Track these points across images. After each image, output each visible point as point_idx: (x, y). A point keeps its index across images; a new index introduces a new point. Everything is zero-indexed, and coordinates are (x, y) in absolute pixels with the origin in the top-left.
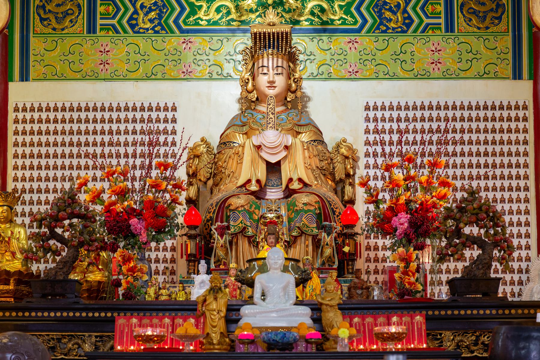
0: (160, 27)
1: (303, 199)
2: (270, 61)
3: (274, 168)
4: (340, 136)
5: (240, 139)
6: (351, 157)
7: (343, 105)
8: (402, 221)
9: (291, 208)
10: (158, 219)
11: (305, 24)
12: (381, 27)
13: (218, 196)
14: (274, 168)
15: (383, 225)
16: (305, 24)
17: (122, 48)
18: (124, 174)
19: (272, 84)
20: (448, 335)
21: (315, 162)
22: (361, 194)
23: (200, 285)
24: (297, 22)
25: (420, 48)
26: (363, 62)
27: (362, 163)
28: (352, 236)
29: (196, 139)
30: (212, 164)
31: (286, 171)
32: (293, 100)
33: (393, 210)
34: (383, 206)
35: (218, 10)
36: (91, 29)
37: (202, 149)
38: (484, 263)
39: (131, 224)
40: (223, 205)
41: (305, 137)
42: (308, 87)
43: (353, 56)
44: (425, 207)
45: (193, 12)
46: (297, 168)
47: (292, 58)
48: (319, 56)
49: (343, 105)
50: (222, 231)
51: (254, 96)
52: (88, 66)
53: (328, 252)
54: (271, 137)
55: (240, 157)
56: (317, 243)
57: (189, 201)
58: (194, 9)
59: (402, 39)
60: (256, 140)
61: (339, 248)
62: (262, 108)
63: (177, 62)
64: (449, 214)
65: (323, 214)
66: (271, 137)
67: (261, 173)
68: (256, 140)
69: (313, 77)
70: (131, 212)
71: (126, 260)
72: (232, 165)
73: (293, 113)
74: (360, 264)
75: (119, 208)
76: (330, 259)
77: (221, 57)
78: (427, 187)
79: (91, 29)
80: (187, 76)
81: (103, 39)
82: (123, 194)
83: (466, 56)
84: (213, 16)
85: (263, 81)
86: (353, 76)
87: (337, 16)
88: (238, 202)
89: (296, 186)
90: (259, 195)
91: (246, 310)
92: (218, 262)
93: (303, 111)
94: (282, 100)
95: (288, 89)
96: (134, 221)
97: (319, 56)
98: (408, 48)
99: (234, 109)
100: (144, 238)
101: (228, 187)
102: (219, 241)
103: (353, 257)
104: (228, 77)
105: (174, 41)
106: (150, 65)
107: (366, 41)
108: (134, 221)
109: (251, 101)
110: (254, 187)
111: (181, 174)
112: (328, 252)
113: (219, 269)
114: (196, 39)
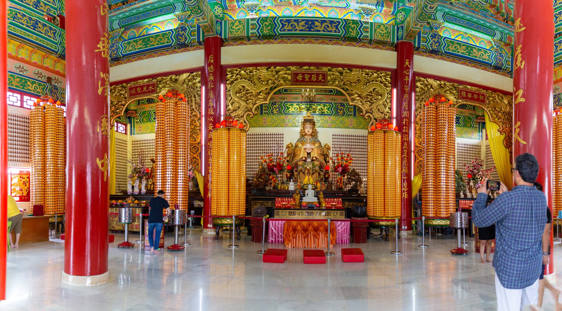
0: (280, 113)
1: (316, 163)
2: (308, 126)
3: (309, 154)
4: (326, 143)
5: (300, 145)
6: (329, 149)
7: (327, 134)
8: (340, 169)
9: (313, 164)
10: (280, 167)
11: (317, 113)
12: (337, 114)
13: (295, 161)
14: (309, 154)
15: (336, 170)
16: (317, 113)
17: (269, 119)
18: (272, 155)
19: (309, 131)
20: (346, 203)
21: (319, 152)
22: (331, 161)
23: (292, 186)
24: (315, 112)
25: (347, 120)
26: (332, 123)
27: (332, 149)
28: (328, 173)
29: (288, 143)
30: (293, 151)
31: (312, 155)
32: (314, 134)
33: (338, 166)
34: (336, 164)
35: (294, 108)
36: (262, 114)
37: (290, 145)
38: (356, 186)
39: (273, 168)
40: (296, 164)
41: (317, 145)
42: (318, 129)
43: (329, 122)
44: (346, 166)
45: (288, 109)
46: (315, 154)
47: (314, 124)
48: (321, 121)
49: (327, 134)
50: (296, 171)
51: (304, 134)
52: (261, 124)
53: (322, 176)
54: (308, 146)
55: (301, 151)
56: (319, 174)
57: (287, 161)
58: (288, 108)
59: (342, 118)
60: (304, 147)
61: (325, 176)
62: (306, 137)
63: (284, 122)
64: (338, 197)
65: (321, 167)
66: (308, 146)
67: (306, 155)
68: (304, 147)
69: (319, 127)
70: (274, 166)
71: (273, 178)
72: (298, 153)
73: (314, 138)
74: (330, 179)
75: (271, 165)
76: (323, 178)
77: (295, 121)
78: (346, 161)
79: (262, 114)
80: (286, 126)
81: (265, 116)
82: (271, 161)
83: (359, 123)
84: (293, 110)
85: (306, 130)
86: (330, 127)
87: (326, 111)
88: (300, 163)
89: (314, 159)
90: (305, 161)
91: (304, 198)
92: (295, 178)
93: (316, 138)
94: (311, 135)
95: (313, 132)
96: (275, 168)
97: (321, 121)
98: (344, 120)
99: (298, 136)
100: (277, 172)
101: (297, 158)
102: (296, 173)
103: (328, 178)
104: (297, 126)
105: (283, 117)
106: (277, 123)
107: (333, 118)
108: (275, 168)
109: (303, 135)
110: (304, 159)
111: (285, 155)
112: (322, 176)
113: (296, 181)
114: (289, 116)
